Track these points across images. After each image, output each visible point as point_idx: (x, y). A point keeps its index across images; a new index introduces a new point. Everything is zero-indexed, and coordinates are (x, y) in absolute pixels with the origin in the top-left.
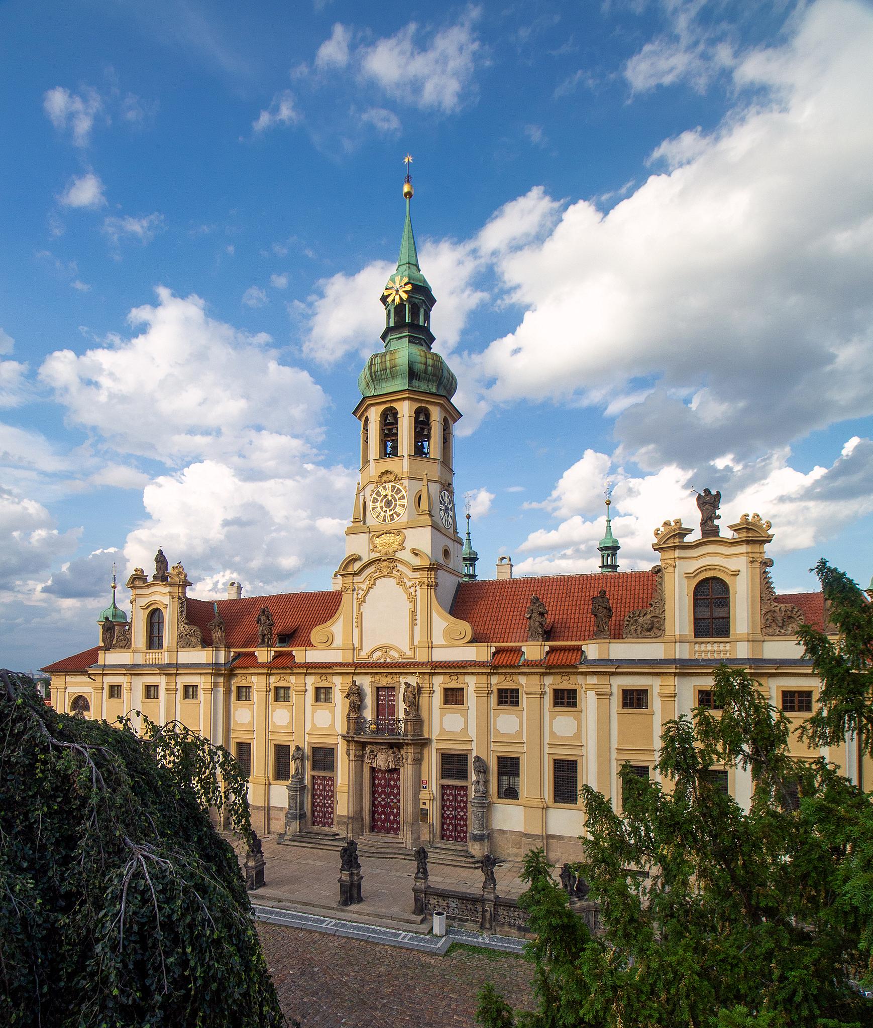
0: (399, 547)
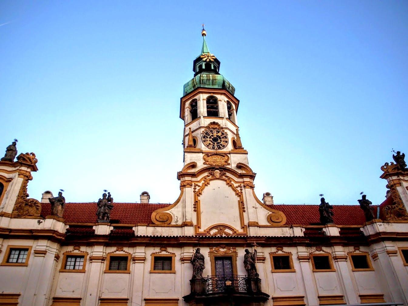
0: (226, 164)
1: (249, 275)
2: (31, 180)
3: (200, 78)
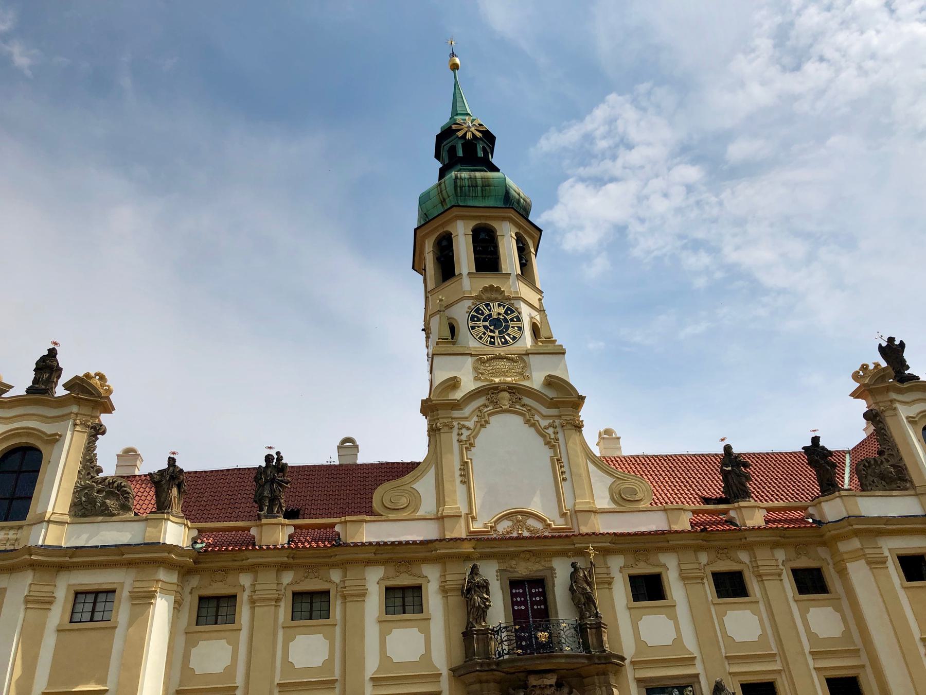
1: (582, 617)
2: (103, 433)
3: (455, 182)
